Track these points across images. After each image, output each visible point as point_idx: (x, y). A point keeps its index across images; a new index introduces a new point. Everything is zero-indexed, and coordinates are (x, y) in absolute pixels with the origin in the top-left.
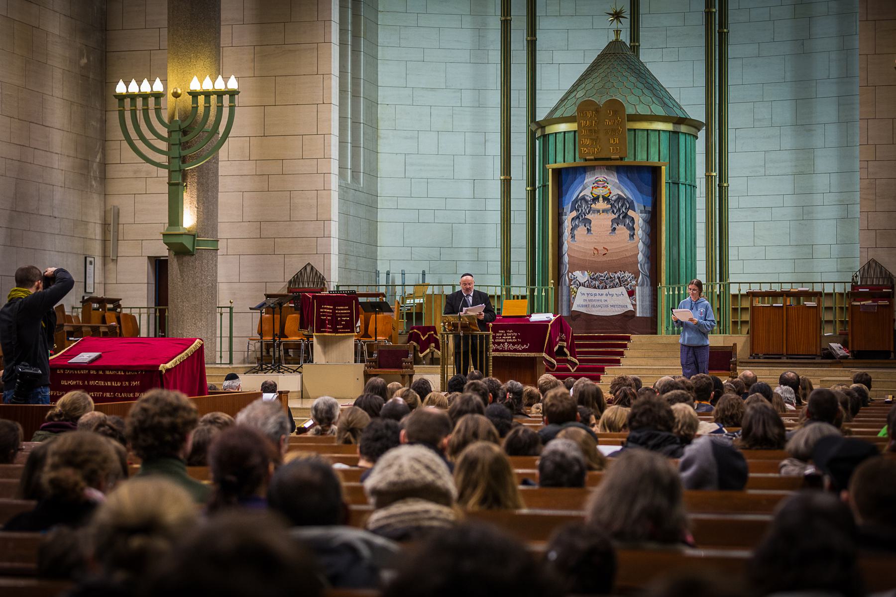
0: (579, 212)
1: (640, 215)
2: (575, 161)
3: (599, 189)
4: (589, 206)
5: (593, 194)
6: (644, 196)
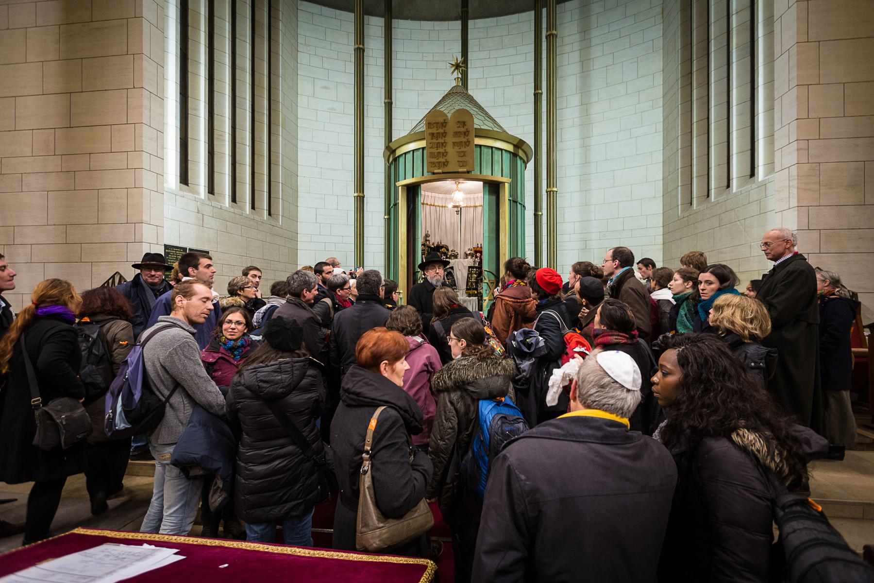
2: (423, 175)
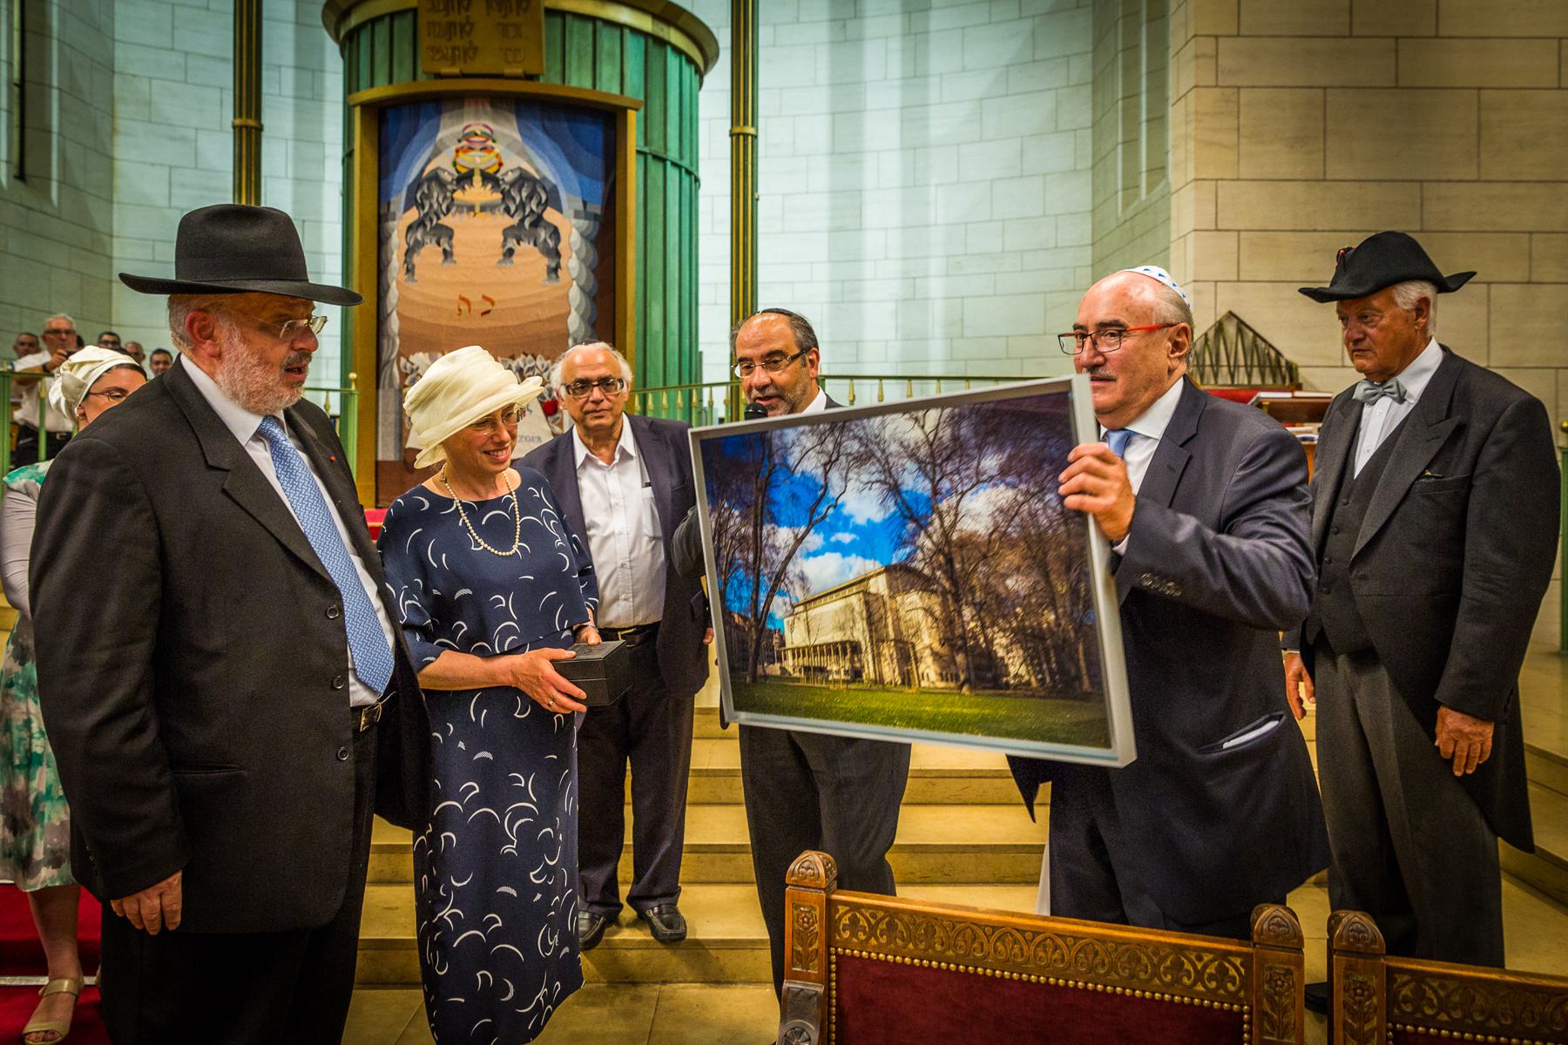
0: (423, 208)
1: (574, 221)
3: (472, 153)
4: (449, 194)
5: (459, 168)
6: (586, 180)
